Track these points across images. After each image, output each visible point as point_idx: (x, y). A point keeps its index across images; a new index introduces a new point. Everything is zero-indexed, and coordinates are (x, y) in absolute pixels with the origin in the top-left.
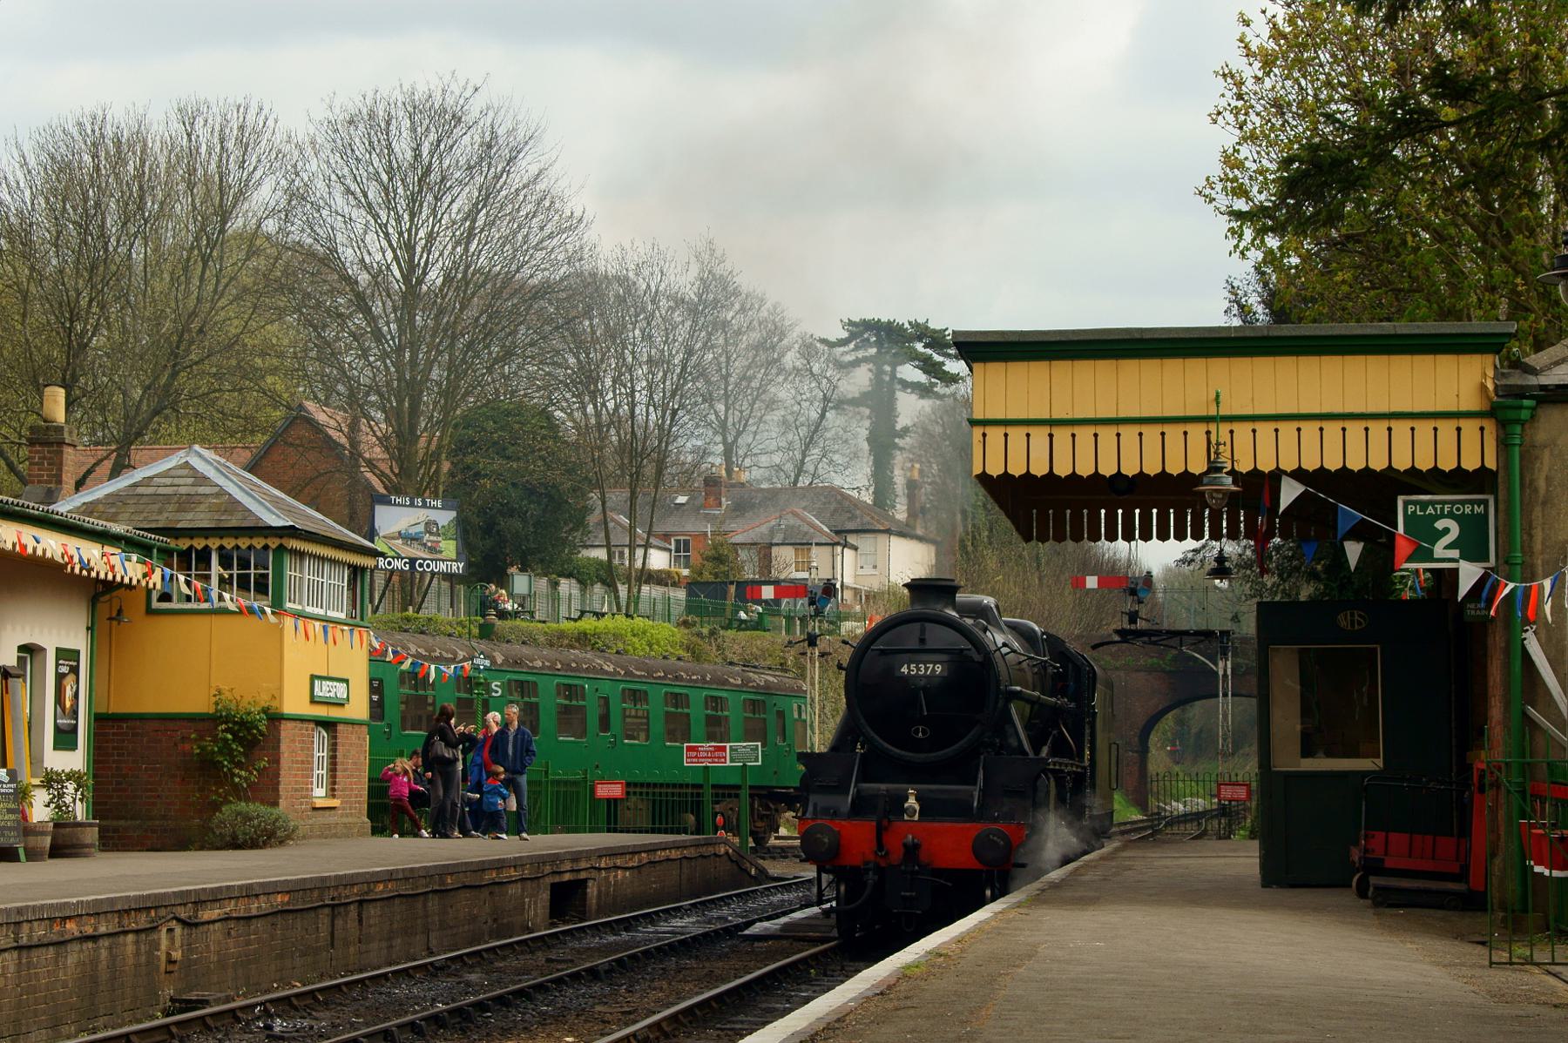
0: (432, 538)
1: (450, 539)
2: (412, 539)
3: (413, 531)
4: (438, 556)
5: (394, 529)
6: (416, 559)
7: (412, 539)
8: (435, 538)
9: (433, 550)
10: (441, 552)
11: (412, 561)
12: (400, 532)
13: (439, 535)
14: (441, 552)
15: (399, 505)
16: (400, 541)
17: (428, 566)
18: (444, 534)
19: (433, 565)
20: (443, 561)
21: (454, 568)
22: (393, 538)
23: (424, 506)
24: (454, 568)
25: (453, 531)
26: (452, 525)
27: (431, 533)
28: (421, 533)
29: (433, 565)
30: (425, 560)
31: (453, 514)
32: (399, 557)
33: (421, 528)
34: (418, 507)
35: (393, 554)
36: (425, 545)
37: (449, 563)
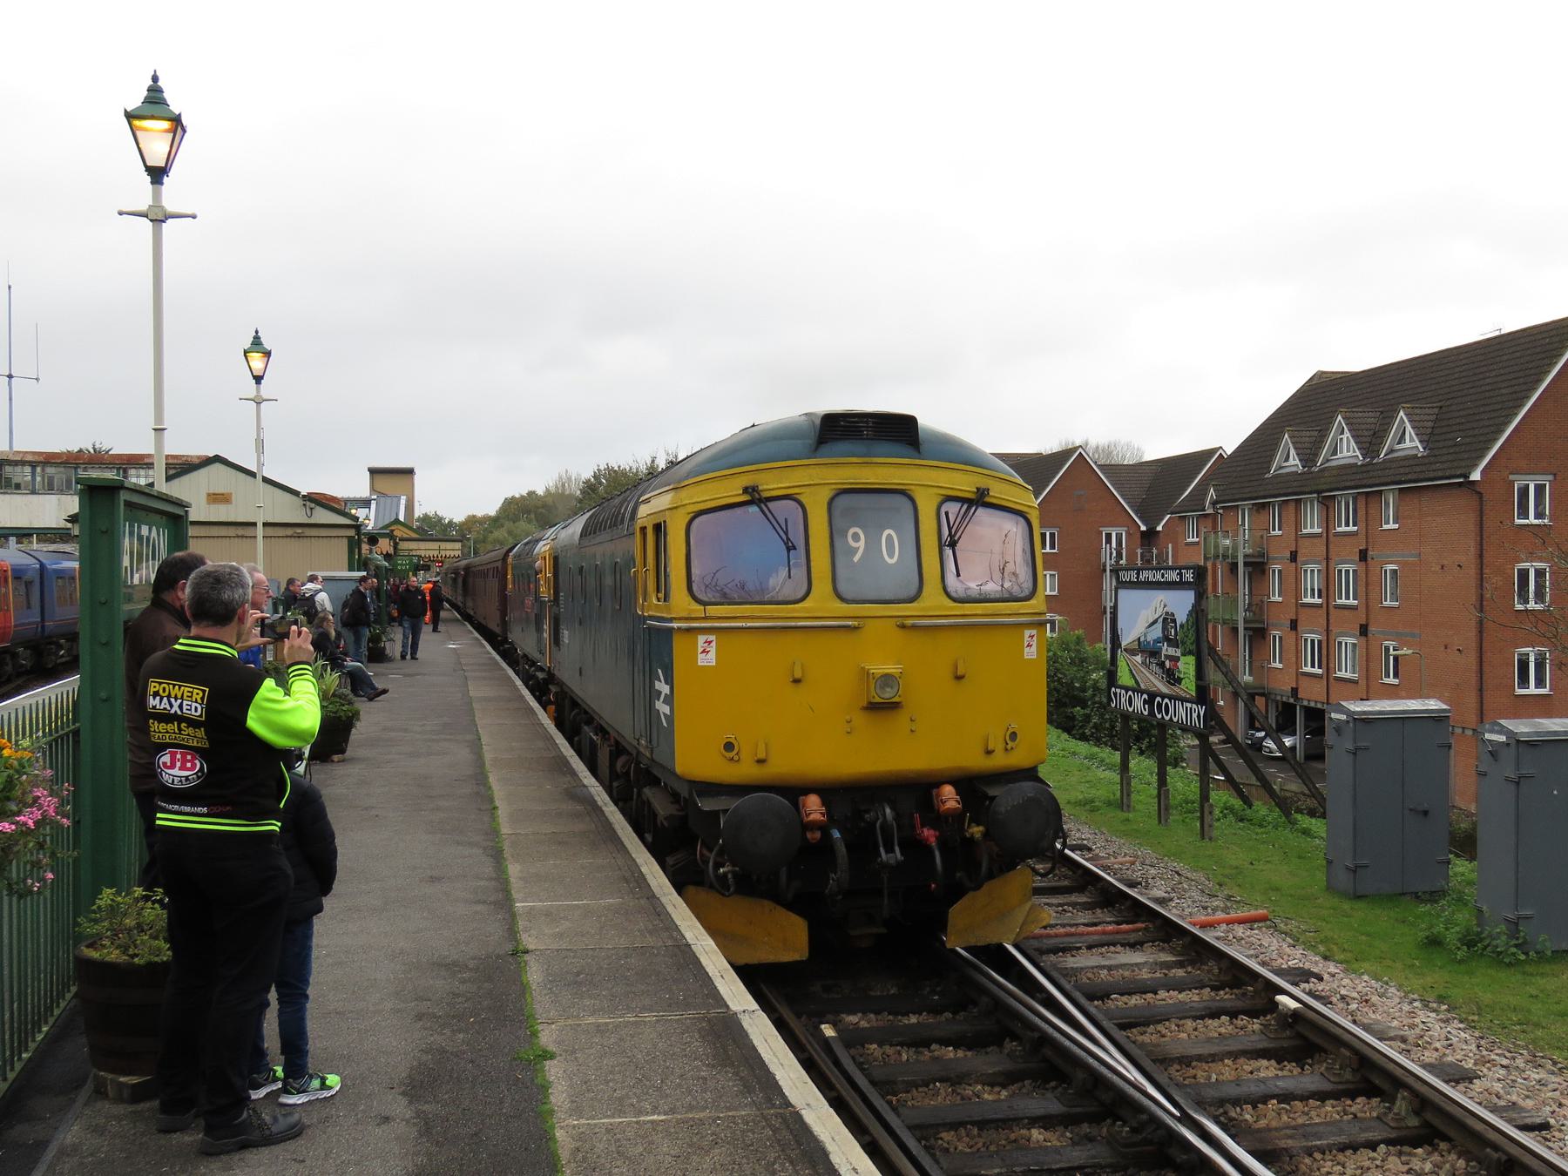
1: (1190, 653)
4: (1176, 690)
10: (1179, 680)
13: (1178, 647)
14: (1179, 680)
16: (1139, 658)
18: (1183, 643)
19: (1171, 710)
20: (1183, 700)
21: (1195, 715)
24: (1195, 715)
26: (1190, 623)
28: (1157, 641)
30: (1163, 696)
32: (1137, 690)
36: (1162, 665)
37: (1189, 705)
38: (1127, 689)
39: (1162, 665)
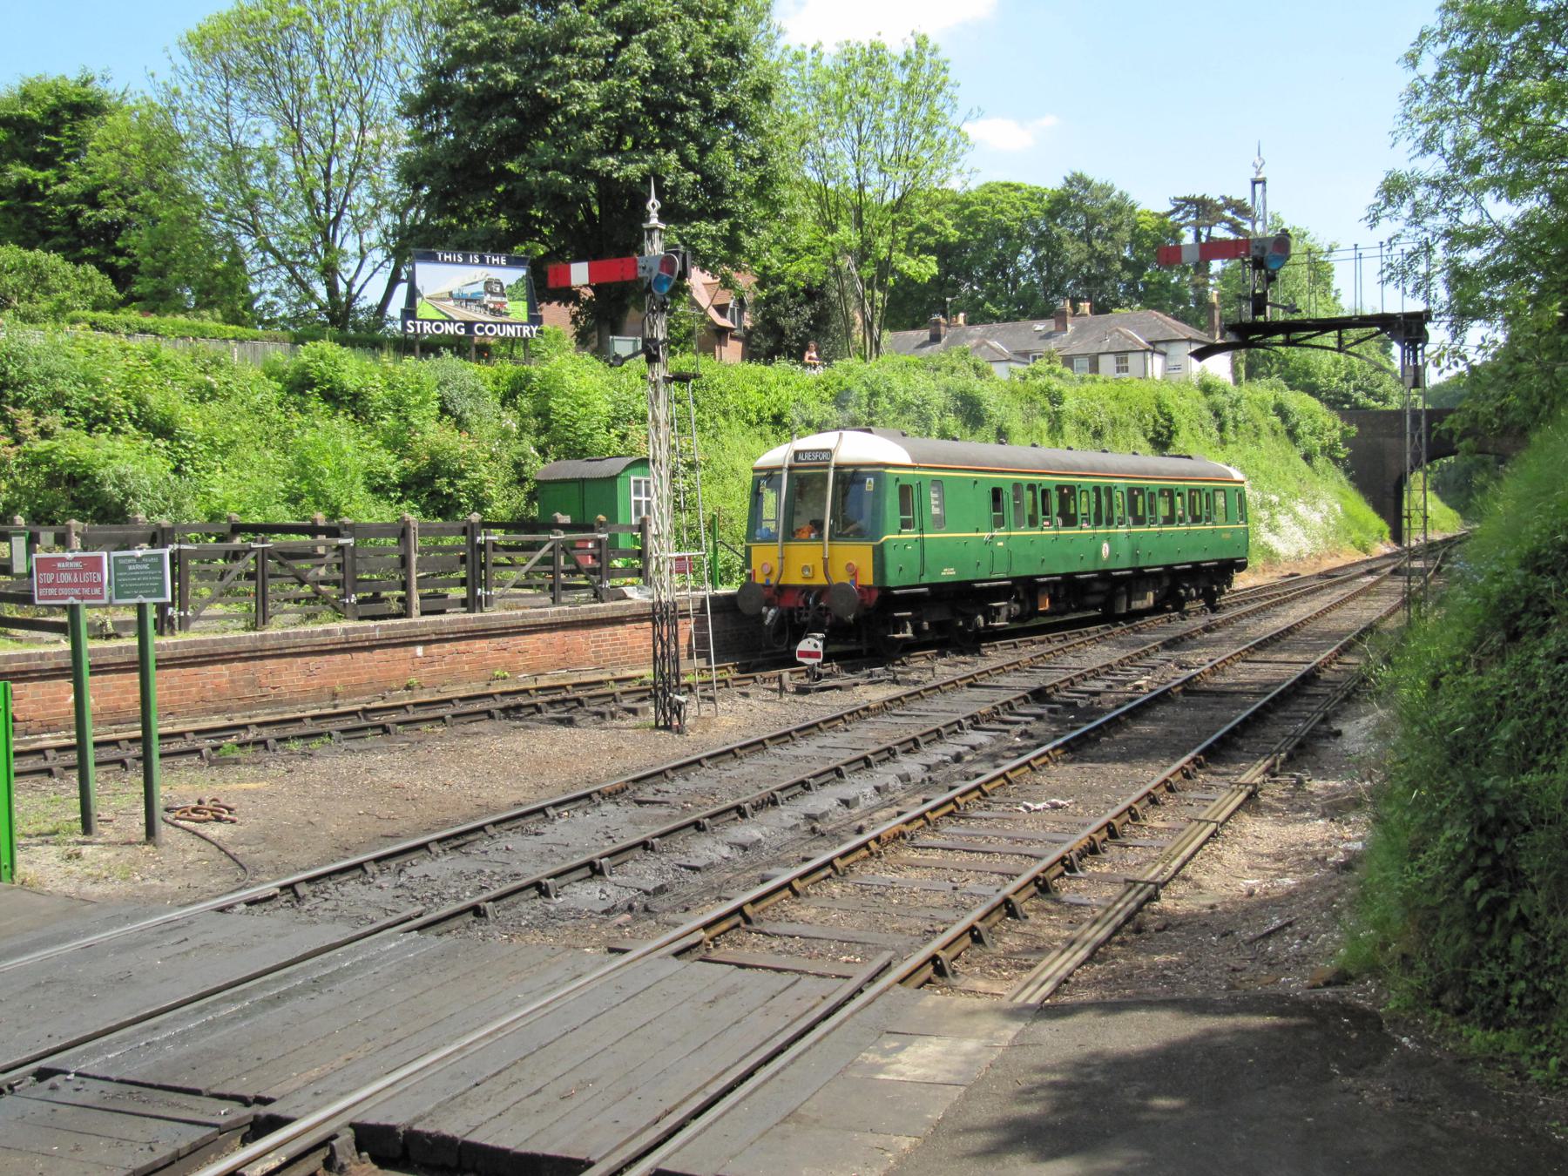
0: (495, 299)
2: (468, 300)
3: (468, 291)
5: (443, 289)
6: (473, 323)
7: (468, 300)
8: (499, 299)
9: (494, 312)
11: (469, 325)
12: (451, 294)
15: (448, 262)
16: (452, 303)
17: (491, 330)
22: (442, 299)
23: (483, 261)
25: (522, 291)
27: (493, 293)
29: (497, 329)
30: (485, 323)
31: (520, 273)
32: (451, 321)
33: (480, 288)
34: (474, 264)
35: (442, 317)
36: (485, 307)
38: (432, 321)
39: (485, 307)
